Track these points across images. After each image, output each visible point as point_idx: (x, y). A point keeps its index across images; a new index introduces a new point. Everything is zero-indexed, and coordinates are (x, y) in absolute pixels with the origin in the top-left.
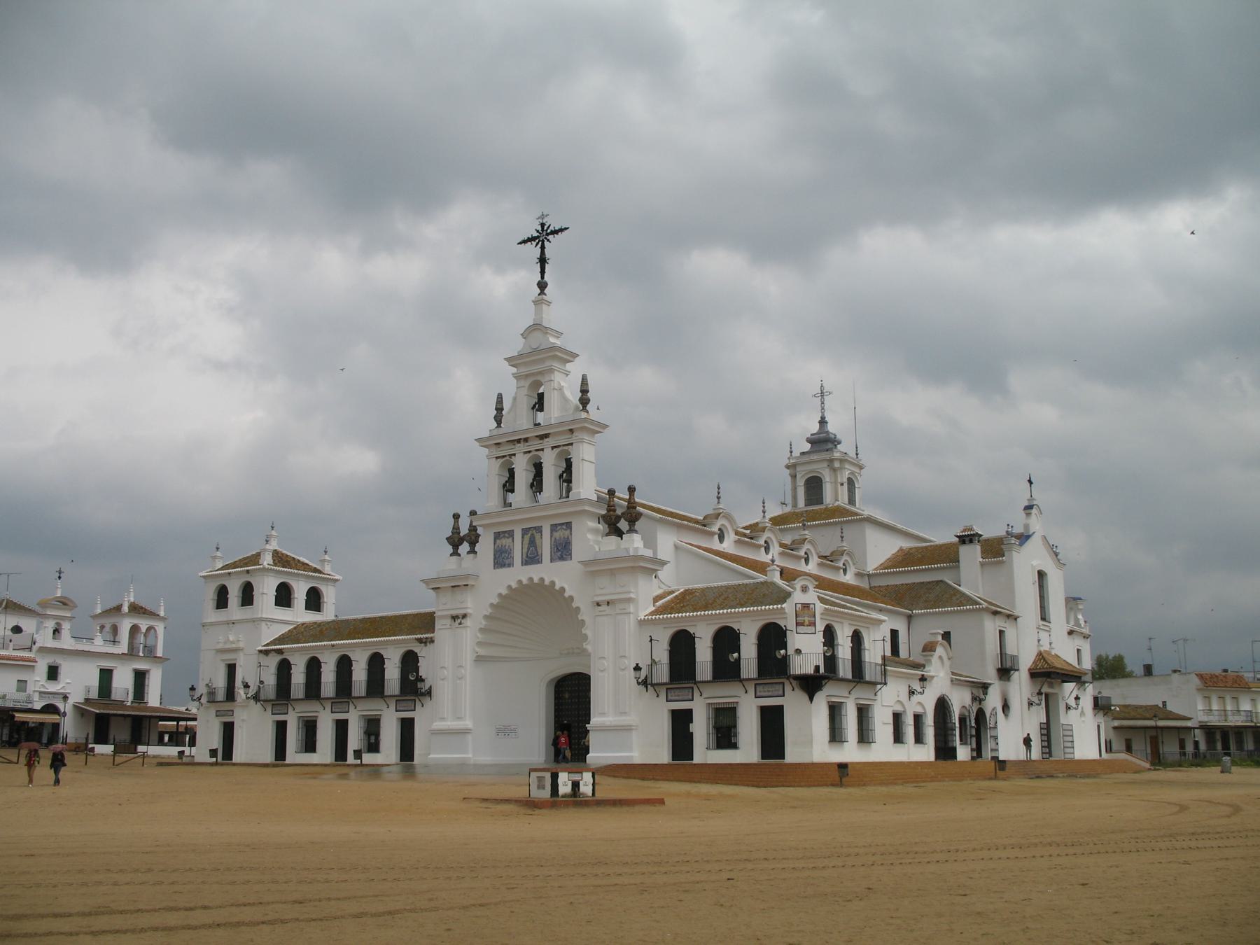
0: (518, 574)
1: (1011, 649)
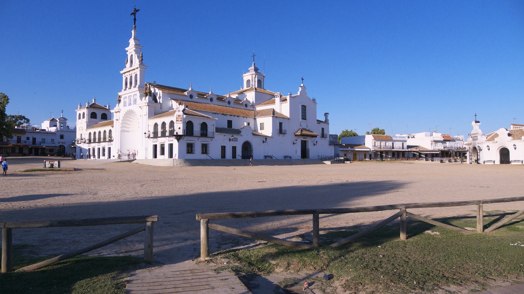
0: (128, 108)
1: (284, 128)
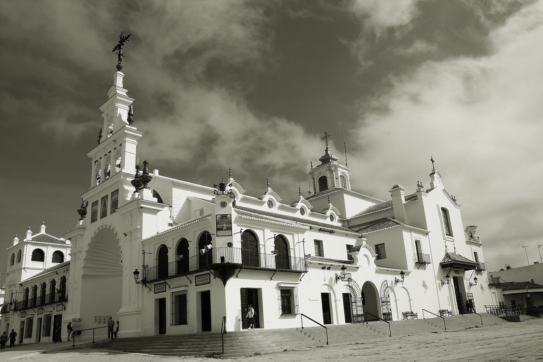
1: (425, 251)
